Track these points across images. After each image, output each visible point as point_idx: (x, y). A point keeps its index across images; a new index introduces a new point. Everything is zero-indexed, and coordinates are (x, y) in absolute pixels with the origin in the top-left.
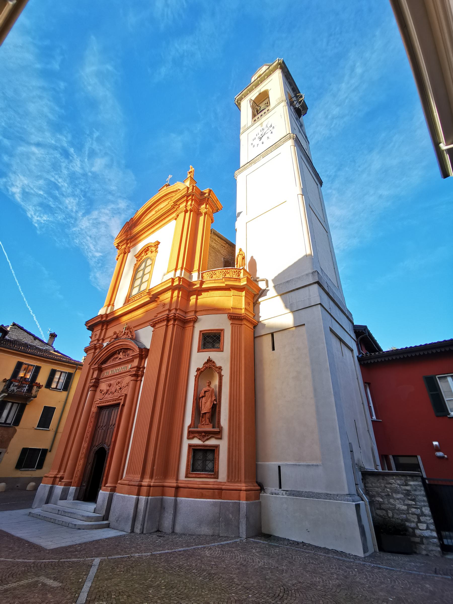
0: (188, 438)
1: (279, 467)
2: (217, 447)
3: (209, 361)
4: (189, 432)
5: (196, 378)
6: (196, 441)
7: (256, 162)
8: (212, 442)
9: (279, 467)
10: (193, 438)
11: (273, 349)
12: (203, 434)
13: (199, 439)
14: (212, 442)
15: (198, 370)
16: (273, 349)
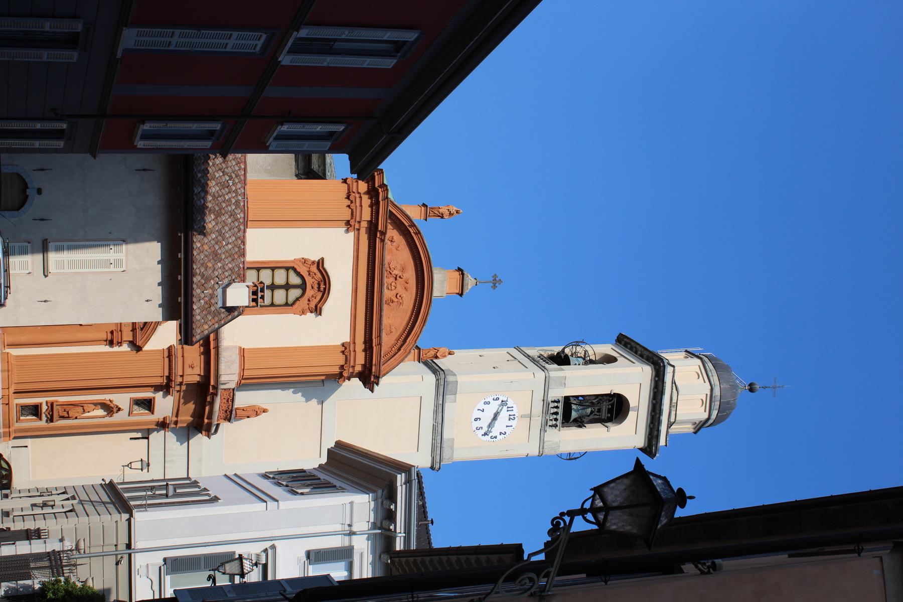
0: (47, 402)
1: (27, 447)
2: (41, 419)
3: (119, 409)
4: (52, 404)
5: (103, 400)
6: (44, 408)
7: (435, 414)
8: (44, 418)
9: (27, 447)
10: (47, 405)
11: (131, 439)
12: (51, 413)
13: (47, 410)
14: (44, 418)
15: (111, 401)
16: (131, 439)
